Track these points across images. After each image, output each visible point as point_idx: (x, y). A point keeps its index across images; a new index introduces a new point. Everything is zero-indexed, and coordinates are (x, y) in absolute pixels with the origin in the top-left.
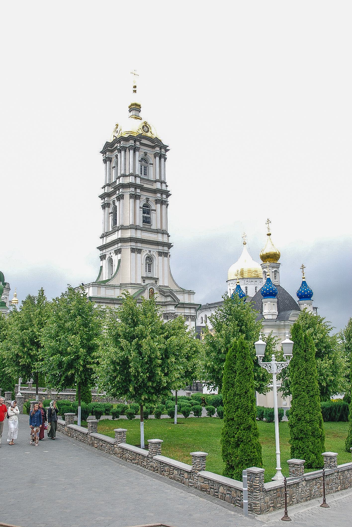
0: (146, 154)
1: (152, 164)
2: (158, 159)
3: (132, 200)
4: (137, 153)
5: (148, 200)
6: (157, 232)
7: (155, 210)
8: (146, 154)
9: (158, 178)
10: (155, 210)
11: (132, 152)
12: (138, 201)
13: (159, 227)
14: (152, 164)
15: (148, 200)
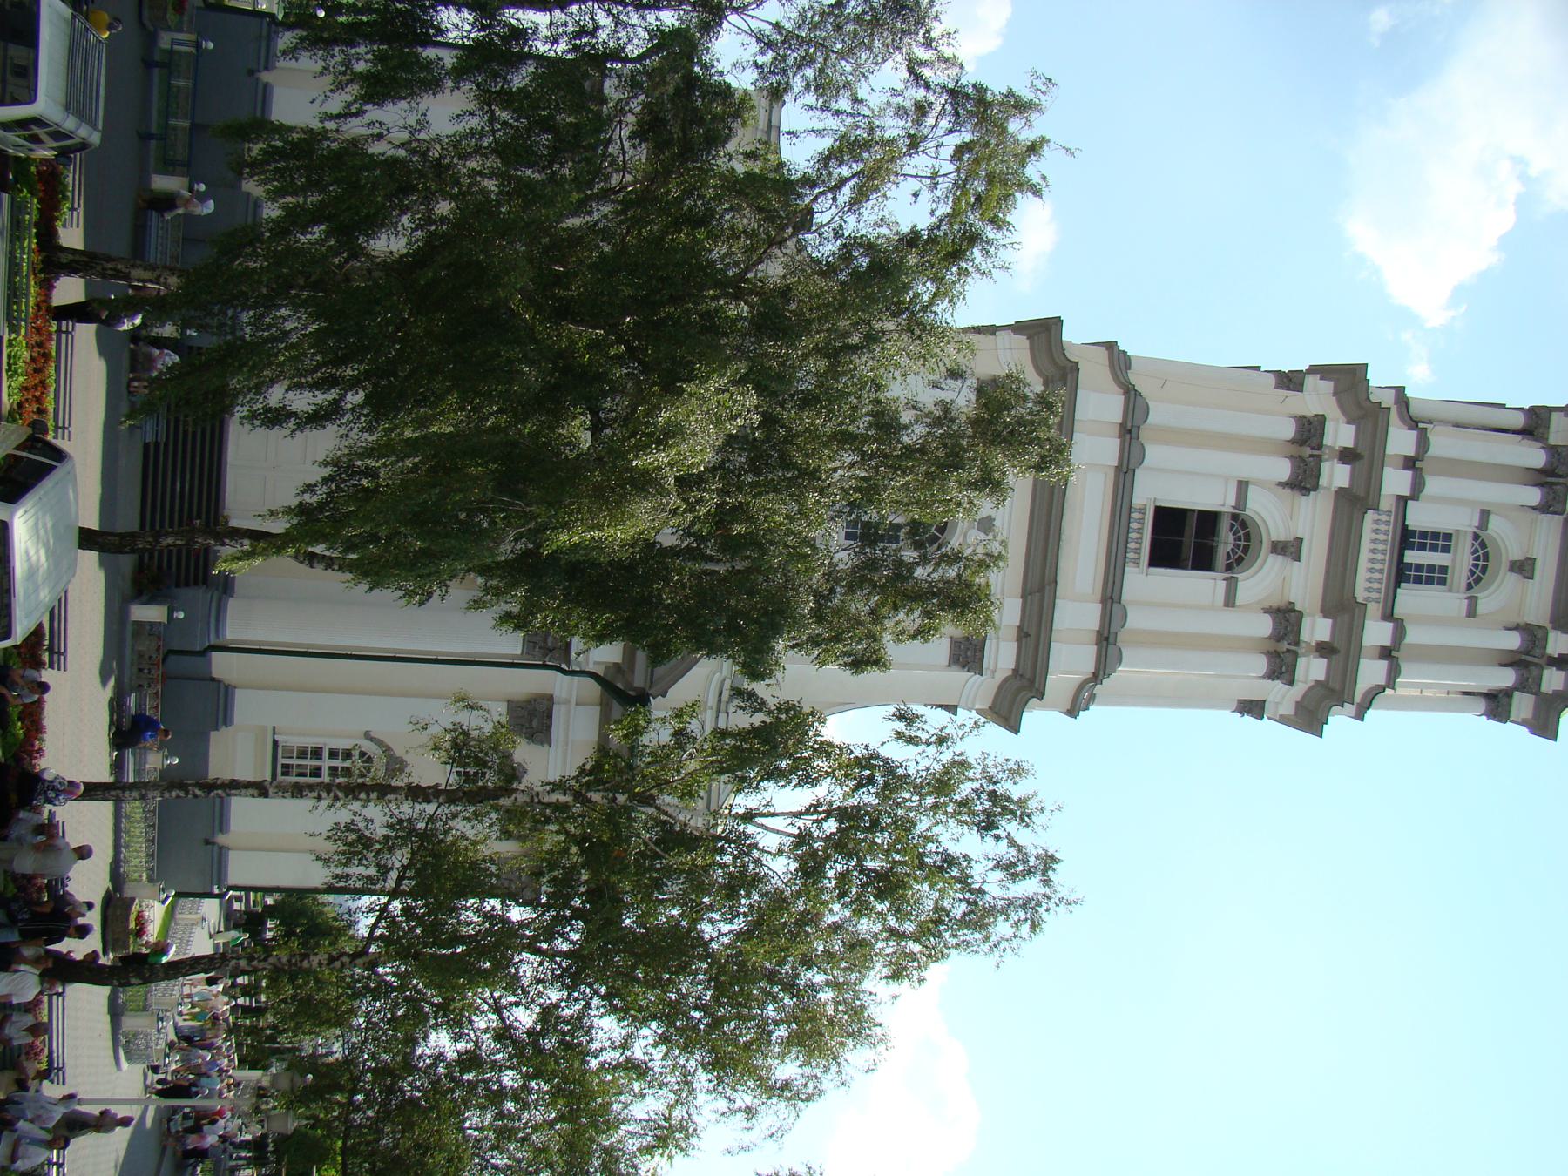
0: (1524, 568)
1: (1472, 613)
2: (1513, 641)
3: (1288, 430)
4: (1533, 496)
5: (1290, 549)
6: (1111, 597)
7: (1230, 601)
8: (1524, 568)
9: (1413, 636)
10: (1230, 601)
11: (1536, 457)
12: (1283, 469)
13: (1137, 620)
14: (1472, 613)
15: (1290, 549)
